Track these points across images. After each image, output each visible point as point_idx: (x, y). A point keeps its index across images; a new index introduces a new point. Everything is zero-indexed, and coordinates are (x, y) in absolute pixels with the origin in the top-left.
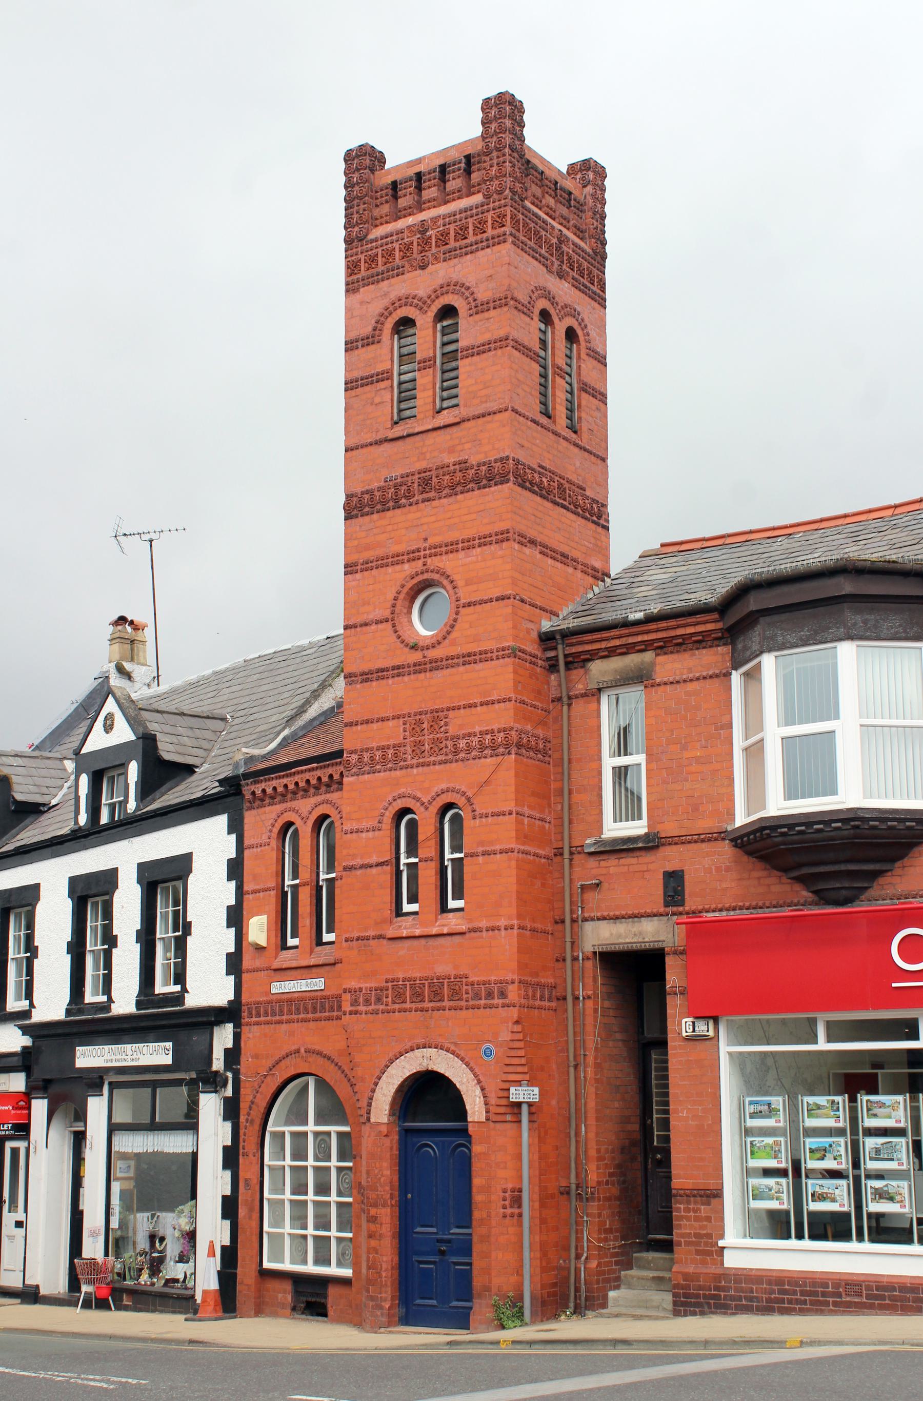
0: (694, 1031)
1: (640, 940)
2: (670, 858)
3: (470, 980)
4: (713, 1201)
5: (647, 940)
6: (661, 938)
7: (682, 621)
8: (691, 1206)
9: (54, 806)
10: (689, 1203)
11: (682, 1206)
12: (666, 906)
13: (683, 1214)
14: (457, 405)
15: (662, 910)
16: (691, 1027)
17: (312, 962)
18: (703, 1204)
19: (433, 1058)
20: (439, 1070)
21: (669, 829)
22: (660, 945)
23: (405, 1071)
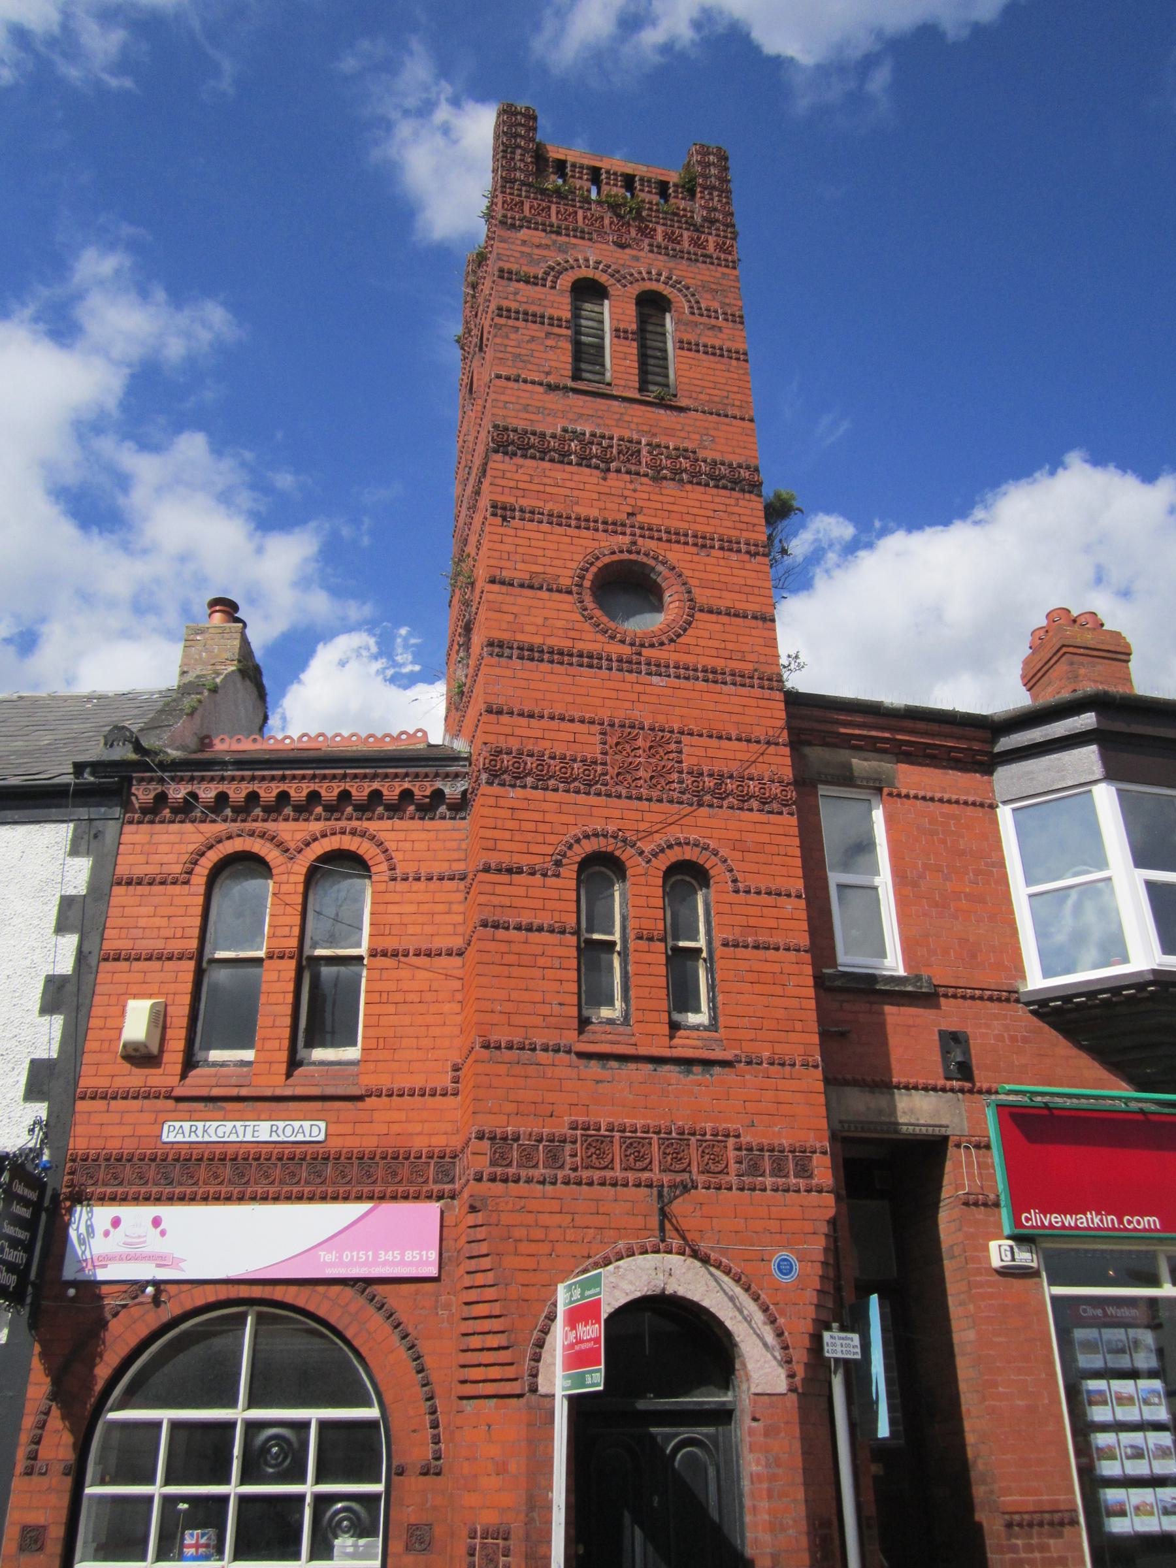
0: (1013, 1259)
1: (913, 1121)
2: (951, 1015)
3: (744, 1140)
4: (1067, 1530)
5: (922, 1122)
6: (944, 1122)
7: (946, 729)
8: (1034, 1541)
9: (681, 409)
10: (1030, 1536)
11: (1019, 1542)
12: (948, 1079)
13: (1023, 1555)
14: (741, 356)
15: (941, 1082)
16: (1009, 1254)
17: (288, 1092)
18: (1052, 1536)
19: (677, 1272)
20: (689, 1296)
21: (941, 974)
22: (943, 1131)
23: (617, 1293)
